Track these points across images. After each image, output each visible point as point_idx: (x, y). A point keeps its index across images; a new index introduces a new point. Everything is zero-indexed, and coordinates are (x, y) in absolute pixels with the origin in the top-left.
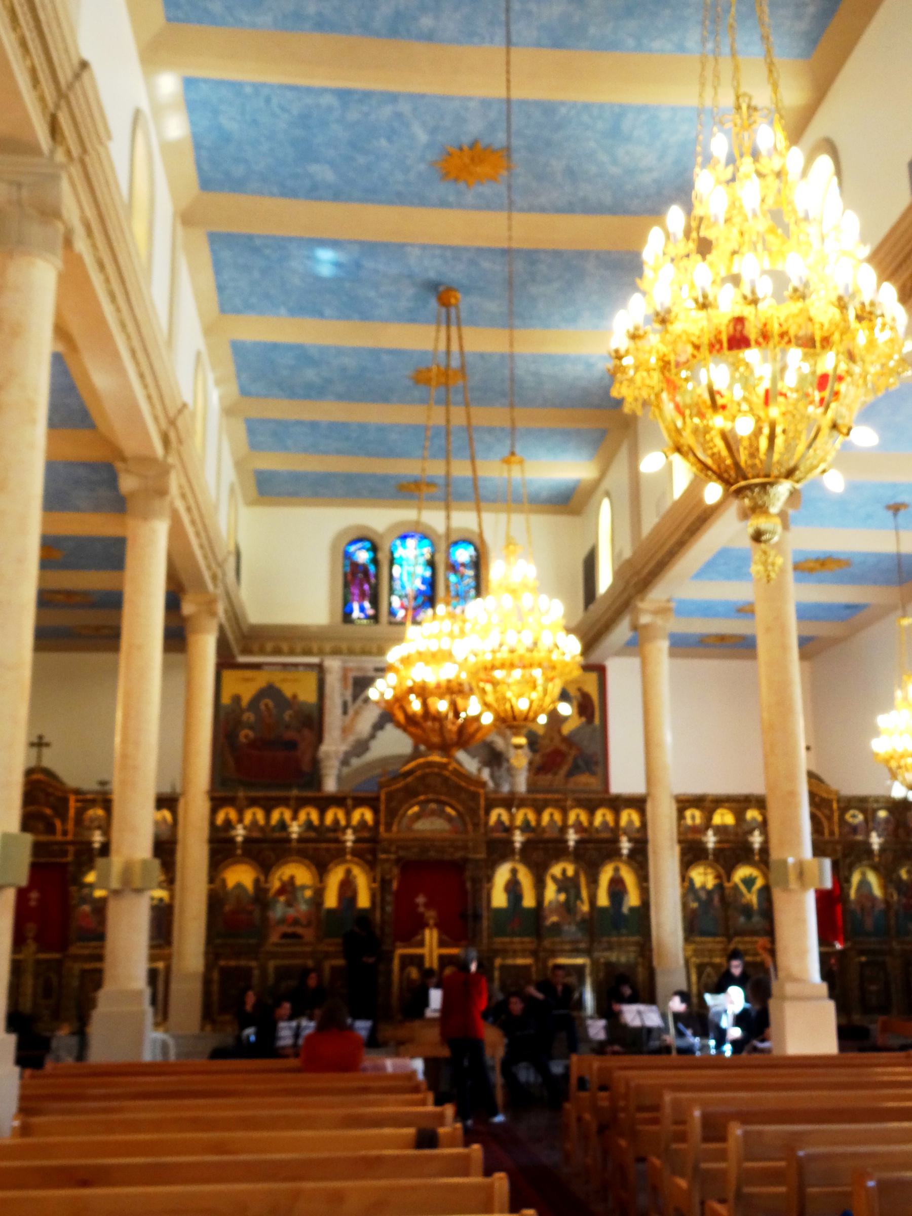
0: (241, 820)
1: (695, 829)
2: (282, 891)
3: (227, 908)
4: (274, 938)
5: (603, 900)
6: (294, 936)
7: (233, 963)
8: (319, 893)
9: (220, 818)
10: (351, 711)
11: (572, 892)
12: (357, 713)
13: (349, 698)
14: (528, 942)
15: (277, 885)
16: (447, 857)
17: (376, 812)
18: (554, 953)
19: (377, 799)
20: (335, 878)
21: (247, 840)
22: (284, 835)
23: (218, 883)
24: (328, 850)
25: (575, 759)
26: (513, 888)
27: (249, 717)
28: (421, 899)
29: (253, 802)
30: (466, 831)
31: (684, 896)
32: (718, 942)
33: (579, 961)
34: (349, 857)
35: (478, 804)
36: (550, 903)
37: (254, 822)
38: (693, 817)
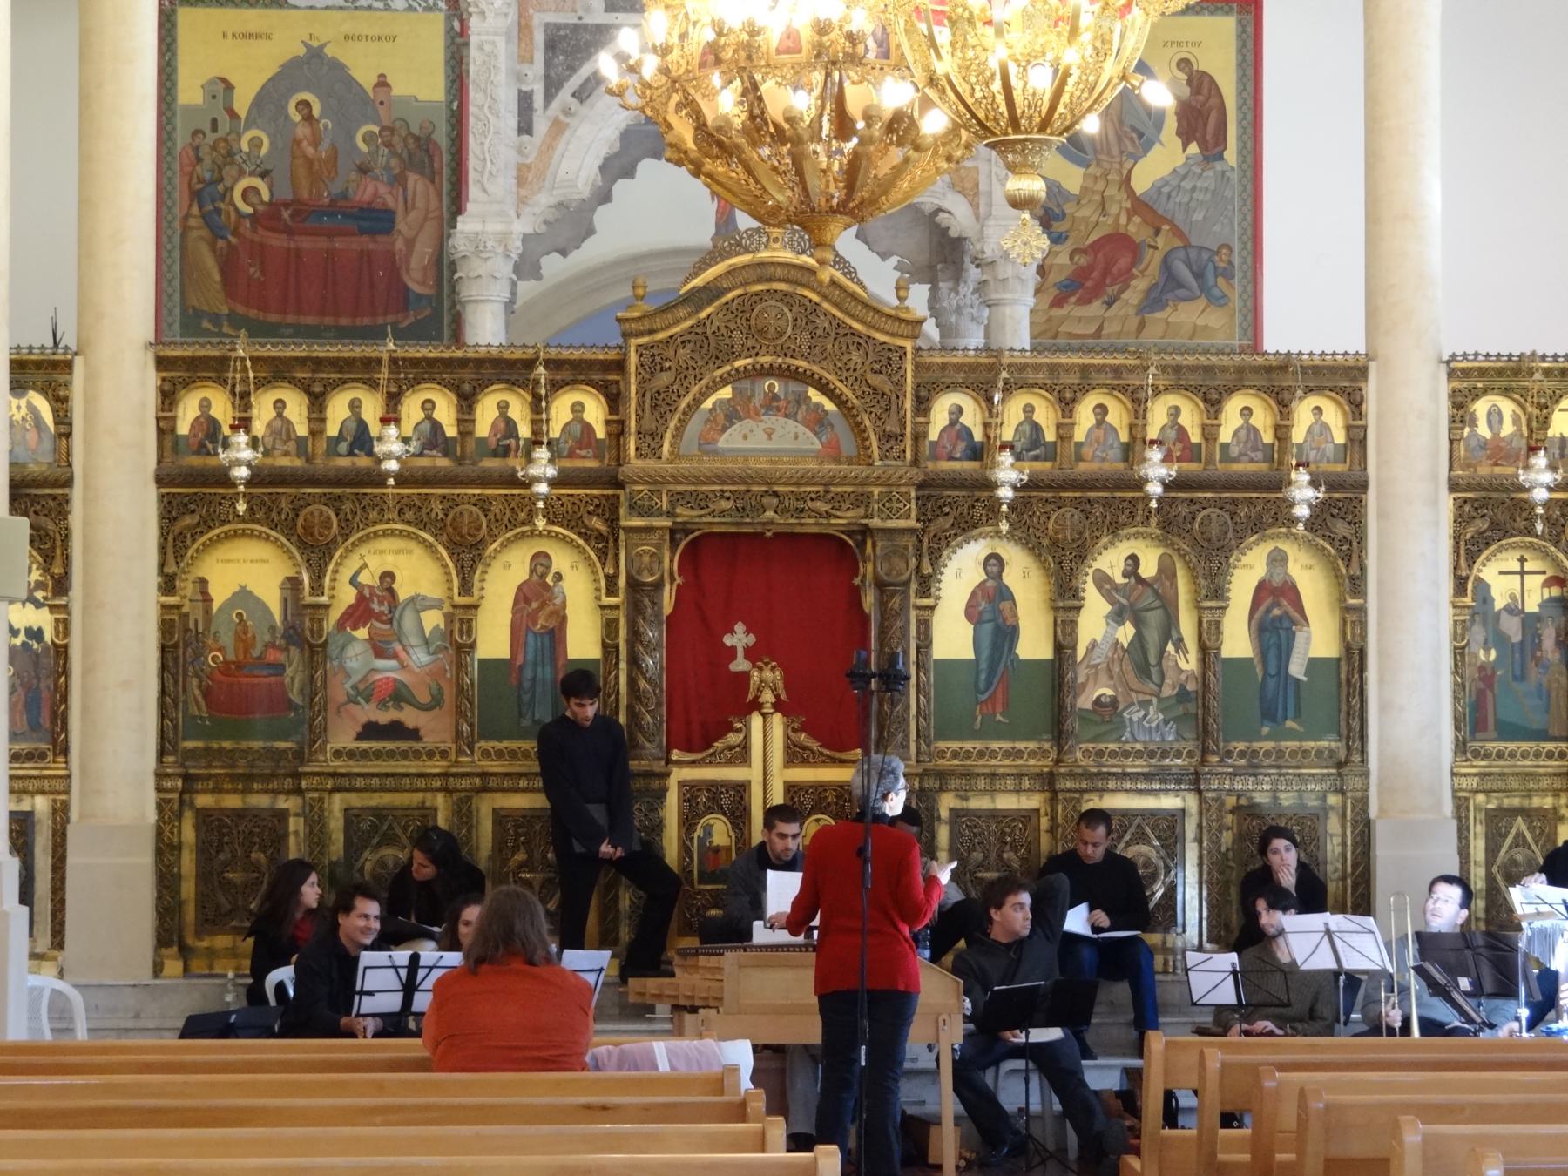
0: (244, 424)
1: (1497, 451)
2: (359, 613)
3: (213, 658)
4: (343, 736)
5: (1237, 642)
6: (395, 730)
7: (233, 801)
8: (462, 619)
10: (541, 125)
11: (1154, 618)
12: (558, 128)
13: (538, 90)
14: (1033, 752)
16: (810, 526)
17: (614, 400)
18: (1099, 780)
19: (620, 366)
21: (259, 477)
22: (363, 462)
23: (187, 588)
24: (483, 504)
25: (1166, 263)
27: (255, 140)
28: (739, 638)
29: (277, 372)
31: (1460, 631)
32: (1550, 755)
33: (1169, 802)
34: (541, 523)
35: (900, 385)
36: (1093, 645)
37: (281, 427)
38: (1495, 417)
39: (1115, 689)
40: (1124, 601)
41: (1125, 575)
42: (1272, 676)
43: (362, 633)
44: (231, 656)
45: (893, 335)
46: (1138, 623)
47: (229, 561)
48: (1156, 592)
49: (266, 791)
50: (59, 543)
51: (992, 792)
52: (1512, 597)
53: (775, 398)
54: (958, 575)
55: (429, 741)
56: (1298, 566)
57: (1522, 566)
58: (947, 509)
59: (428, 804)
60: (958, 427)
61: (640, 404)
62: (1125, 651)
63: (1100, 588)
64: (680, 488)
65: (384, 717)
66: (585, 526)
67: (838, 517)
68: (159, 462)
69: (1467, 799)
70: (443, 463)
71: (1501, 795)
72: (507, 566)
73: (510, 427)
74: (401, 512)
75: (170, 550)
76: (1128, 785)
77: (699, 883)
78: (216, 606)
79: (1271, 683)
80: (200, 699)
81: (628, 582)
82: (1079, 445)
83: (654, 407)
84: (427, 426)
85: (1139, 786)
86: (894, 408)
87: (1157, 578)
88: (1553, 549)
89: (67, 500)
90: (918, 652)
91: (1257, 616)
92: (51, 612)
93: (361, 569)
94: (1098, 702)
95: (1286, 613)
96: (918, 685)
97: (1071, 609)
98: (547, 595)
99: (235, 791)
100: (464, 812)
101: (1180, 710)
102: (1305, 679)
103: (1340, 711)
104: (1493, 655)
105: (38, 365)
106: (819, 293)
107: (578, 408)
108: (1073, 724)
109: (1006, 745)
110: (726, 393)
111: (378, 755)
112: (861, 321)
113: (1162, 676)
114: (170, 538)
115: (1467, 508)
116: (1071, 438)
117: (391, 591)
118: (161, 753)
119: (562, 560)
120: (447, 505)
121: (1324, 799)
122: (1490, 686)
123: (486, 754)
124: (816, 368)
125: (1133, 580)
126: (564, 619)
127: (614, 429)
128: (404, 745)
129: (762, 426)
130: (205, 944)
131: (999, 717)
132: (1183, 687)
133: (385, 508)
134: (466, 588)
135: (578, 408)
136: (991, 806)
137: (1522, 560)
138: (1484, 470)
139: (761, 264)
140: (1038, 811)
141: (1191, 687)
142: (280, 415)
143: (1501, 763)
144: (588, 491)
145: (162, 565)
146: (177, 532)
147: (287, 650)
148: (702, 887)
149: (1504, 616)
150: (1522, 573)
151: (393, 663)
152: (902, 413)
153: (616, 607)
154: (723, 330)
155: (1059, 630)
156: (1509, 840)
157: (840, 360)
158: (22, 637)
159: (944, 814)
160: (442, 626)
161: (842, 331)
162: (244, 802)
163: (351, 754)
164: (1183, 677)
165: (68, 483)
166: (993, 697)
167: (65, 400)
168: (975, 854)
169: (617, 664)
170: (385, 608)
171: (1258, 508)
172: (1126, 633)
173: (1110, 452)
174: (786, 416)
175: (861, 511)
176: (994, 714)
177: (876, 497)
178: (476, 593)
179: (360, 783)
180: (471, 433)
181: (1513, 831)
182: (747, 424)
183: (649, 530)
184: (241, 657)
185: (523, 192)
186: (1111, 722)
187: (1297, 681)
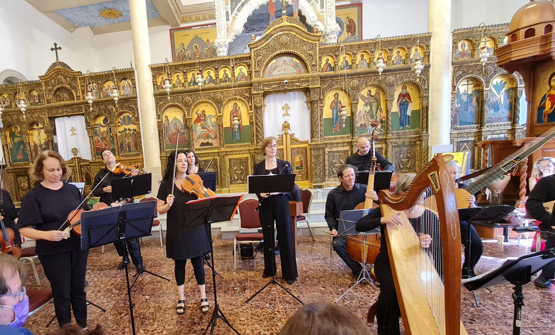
1: (463, 54)
5: (395, 108)
8: (219, 118)
9: (159, 80)
11: (375, 104)
15: (195, 117)
20: (228, 109)
26: (336, 106)
36: (360, 112)
46: (371, 106)
48: (375, 98)
52: (465, 90)
54: (328, 99)
63: (361, 99)
68: (154, 91)
69: (454, 140)
70: (213, 85)
72: (228, 107)
74: (205, 97)
79: (403, 117)
81: (254, 107)
84: (209, 77)
87: (375, 95)
89: (137, 101)
91: (399, 102)
94: (361, 125)
100: (222, 160)
103: (419, 122)
104: (459, 105)
107: (241, 70)
108: (356, 130)
120: (214, 94)
121: (415, 142)
122: (459, 113)
127: (249, 73)
132: (381, 120)
134: (220, 112)
137: (468, 81)
142: (178, 79)
143: (461, 130)
145: (157, 113)
149: (463, 95)
150: (468, 84)
155: (353, 109)
156: (463, 148)
165: (136, 98)
166: (337, 126)
167: (134, 80)
180: (218, 78)
181: (463, 147)
187: (409, 116)
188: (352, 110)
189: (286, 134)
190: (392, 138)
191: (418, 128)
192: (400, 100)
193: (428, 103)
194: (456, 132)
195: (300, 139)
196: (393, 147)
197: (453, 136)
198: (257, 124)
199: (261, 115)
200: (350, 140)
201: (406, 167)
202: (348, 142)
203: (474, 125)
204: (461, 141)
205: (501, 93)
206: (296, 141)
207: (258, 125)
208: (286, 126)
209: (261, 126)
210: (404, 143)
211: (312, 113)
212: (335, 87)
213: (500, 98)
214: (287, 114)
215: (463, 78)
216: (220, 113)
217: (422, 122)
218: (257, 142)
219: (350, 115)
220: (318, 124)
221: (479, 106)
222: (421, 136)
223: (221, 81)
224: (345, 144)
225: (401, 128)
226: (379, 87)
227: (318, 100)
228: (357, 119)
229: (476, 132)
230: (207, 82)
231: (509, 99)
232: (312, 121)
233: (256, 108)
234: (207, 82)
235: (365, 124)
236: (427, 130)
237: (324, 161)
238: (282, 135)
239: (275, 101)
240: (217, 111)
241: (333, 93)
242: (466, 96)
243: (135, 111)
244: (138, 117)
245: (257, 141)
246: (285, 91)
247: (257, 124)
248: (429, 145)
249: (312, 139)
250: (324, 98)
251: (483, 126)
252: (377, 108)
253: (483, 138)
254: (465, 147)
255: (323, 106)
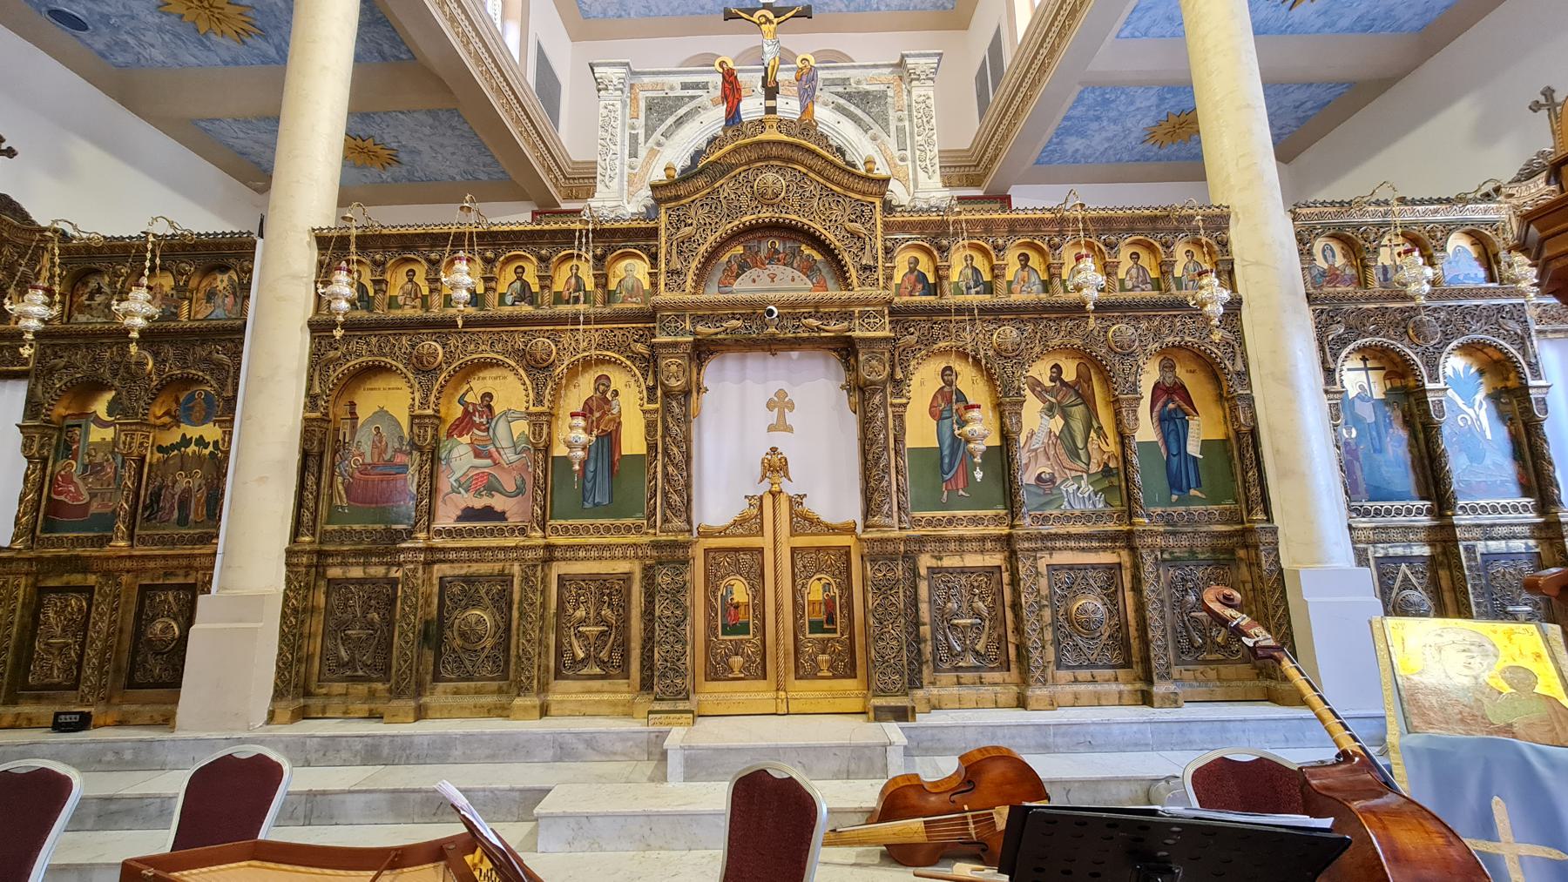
4: (446, 518)
5: (1146, 430)
6: (488, 513)
7: (356, 572)
11: (1078, 412)
17: (654, 258)
19: (653, 233)
26: (950, 403)
30: (847, 286)
36: (1032, 433)
39: (1053, 469)
40: (1053, 400)
41: (1052, 380)
42: (1174, 456)
43: (466, 439)
44: (368, 460)
45: (864, 194)
47: (372, 389)
48: (1077, 392)
49: (381, 564)
50: (232, 374)
51: (961, 553)
52: (1361, 387)
53: (777, 252)
54: (922, 383)
55: (513, 520)
56: (1183, 371)
57: (1365, 364)
58: (912, 330)
59: (506, 572)
60: (916, 273)
61: (669, 253)
62: (1057, 438)
63: (1033, 391)
64: (699, 313)
65: (478, 503)
66: (632, 352)
67: (827, 331)
69: (1365, 550)
70: (525, 309)
71: (1385, 545)
73: (579, 285)
75: (316, 377)
76: (1072, 544)
77: (723, 634)
78: (360, 422)
79: (1175, 460)
80: (342, 492)
82: (1010, 283)
83: (680, 253)
84: (518, 284)
85: (1081, 545)
86: (868, 247)
87: (1077, 382)
88: (1400, 345)
90: (895, 441)
92: (221, 427)
93: (467, 391)
94: (1039, 478)
95: (1179, 406)
96: (897, 468)
97: (1016, 403)
98: (606, 407)
99: (358, 564)
101: (1106, 484)
102: (1201, 457)
103: (1235, 480)
104: (1354, 434)
105: (230, 246)
106: (805, 166)
108: (1024, 495)
109: (970, 513)
110: (739, 250)
111: (471, 533)
112: (838, 184)
113: (1089, 458)
114: (318, 367)
115: (1324, 317)
116: (1003, 276)
117: (490, 408)
118: (296, 533)
119: (618, 379)
121: (1232, 551)
123: (555, 530)
124: (805, 221)
125: (1058, 383)
126: (620, 423)
128: (490, 525)
129: (767, 272)
130: (324, 691)
131: (961, 492)
132: (1106, 465)
133: (480, 342)
135: (629, 268)
136: (961, 564)
137: (1364, 359)
138: (1328, 289)
139: (760, 143)
140: (1000, 567)
141: (1112, 465)
142: (411, 280)
144: (634, 325)
145: (309, 388)
146: (324, 364)
147: (411, 453)
148: (726, 638)
150: (1366, 369)
151: (489, 461)
152: (874, 252)
153: (656, 411)
154: (733, 196)
157: (824, 214)
158: (211, 448)
159: (923, 572)
160: (527, 432)
161: (825, 193)
162: (365, 573)
163: (450, 533)
164: (1106, 457)
167: (250, 271)
168: (950, 605)
169: (656, 456)
170: (484, 420)
171: (1156, 323)
172: (1057, 424)
173: (1034, 288)
174: (785, 265)
175: (846, 323)
176: (958, 490)
177: (857, 315)
178: (547, 403)
179: (453, 556)
182: (754, 272)
183: (675, 345)
184: (376, 460)
185: (631, 189)
186: (1051, 494)
187: (1195, 458)
188: (1002, 425)
189: (773, 494)
190: (1152, 534)
191: (1231, 501)
192: (1159, 405)
193: (1254, 418)
194: (1362, 522)
195: (827, 517)
196: (1157, 563)
197: (1362, 535)
198: (666, 452)
199: (686, 419)
200: (1006, 531)
201: (1213, 642)
202: (998, 539)
203: (1419, 504)
204: (1386, 557)
205: (1477, 403)
206: (811, 522)
207: (669, 456)
208: (775, 466)
209: (679, 457)
210: (1192, 552)
211: (866, 424)
212: (942, 344)
213: (1478, 419)
214: (781, 426)
215: (1351, 347)
216: (541, 403)
217: (1245, 481)
218: (666, 520)
219: (997, 442)
220: (888, 466)
221: (1416, 439)
222: (1252, 530)
223: (558, 299)
224: (989, 545)
225: (1175, 497)
226: (1088, 360)
227: (884, 383)
228: (1023, 457)
229: (1430, 527)
230: (509, 299)
231: (1505, 424)
232: (864, 453)
233: (668, 394)
234: (509, 299)
235: (1052, 480)
236: (1267, 511)
237: (914, 602)
238: (761, 498)
239: (742, 379)
240: (531, 396)
241: (937, 365)
242: (1369, 406)
243: (228, 375)
244: (235, 397)
245: (664, 514)
246: (772, 346)
247: (666, 452)
248: (1284, 564)
249: (865, 518)
250: (906, 377)
251: (1451, 506)
252: (1088, 427)
253: (1461, 548)
254: (1406, 578)
255: (905, 405)
